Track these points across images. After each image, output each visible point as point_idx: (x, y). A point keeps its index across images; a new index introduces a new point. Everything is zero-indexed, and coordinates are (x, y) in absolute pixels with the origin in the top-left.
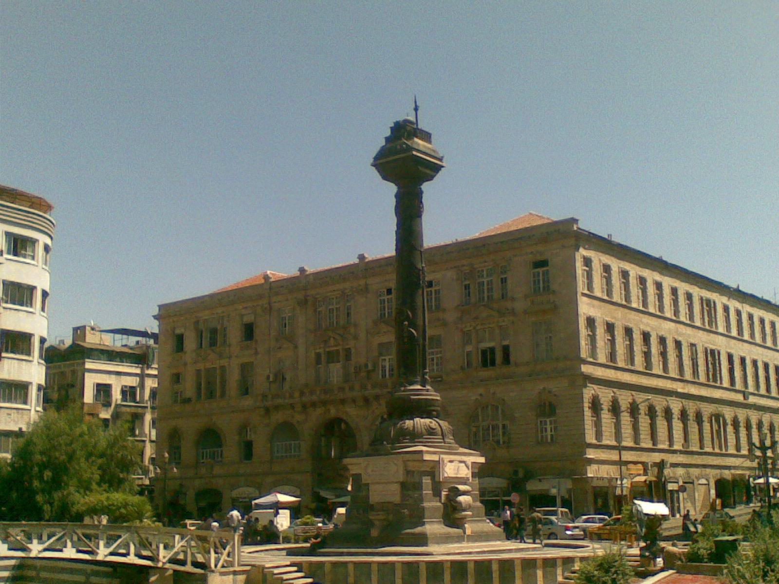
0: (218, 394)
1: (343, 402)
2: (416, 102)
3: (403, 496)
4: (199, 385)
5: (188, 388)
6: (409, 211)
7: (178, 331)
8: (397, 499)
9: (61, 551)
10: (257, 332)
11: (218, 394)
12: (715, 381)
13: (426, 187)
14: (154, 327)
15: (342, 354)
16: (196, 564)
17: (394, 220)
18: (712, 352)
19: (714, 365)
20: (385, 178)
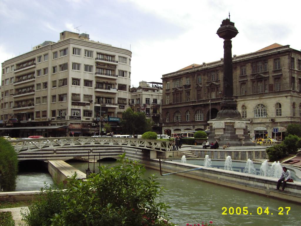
3: (224, 133)
6: (228, 47)
8: (222, 133)
9: (127, 145)
13: (233, 40)
16: (162, 150)
17: (223, 50)
20: (220, 37)
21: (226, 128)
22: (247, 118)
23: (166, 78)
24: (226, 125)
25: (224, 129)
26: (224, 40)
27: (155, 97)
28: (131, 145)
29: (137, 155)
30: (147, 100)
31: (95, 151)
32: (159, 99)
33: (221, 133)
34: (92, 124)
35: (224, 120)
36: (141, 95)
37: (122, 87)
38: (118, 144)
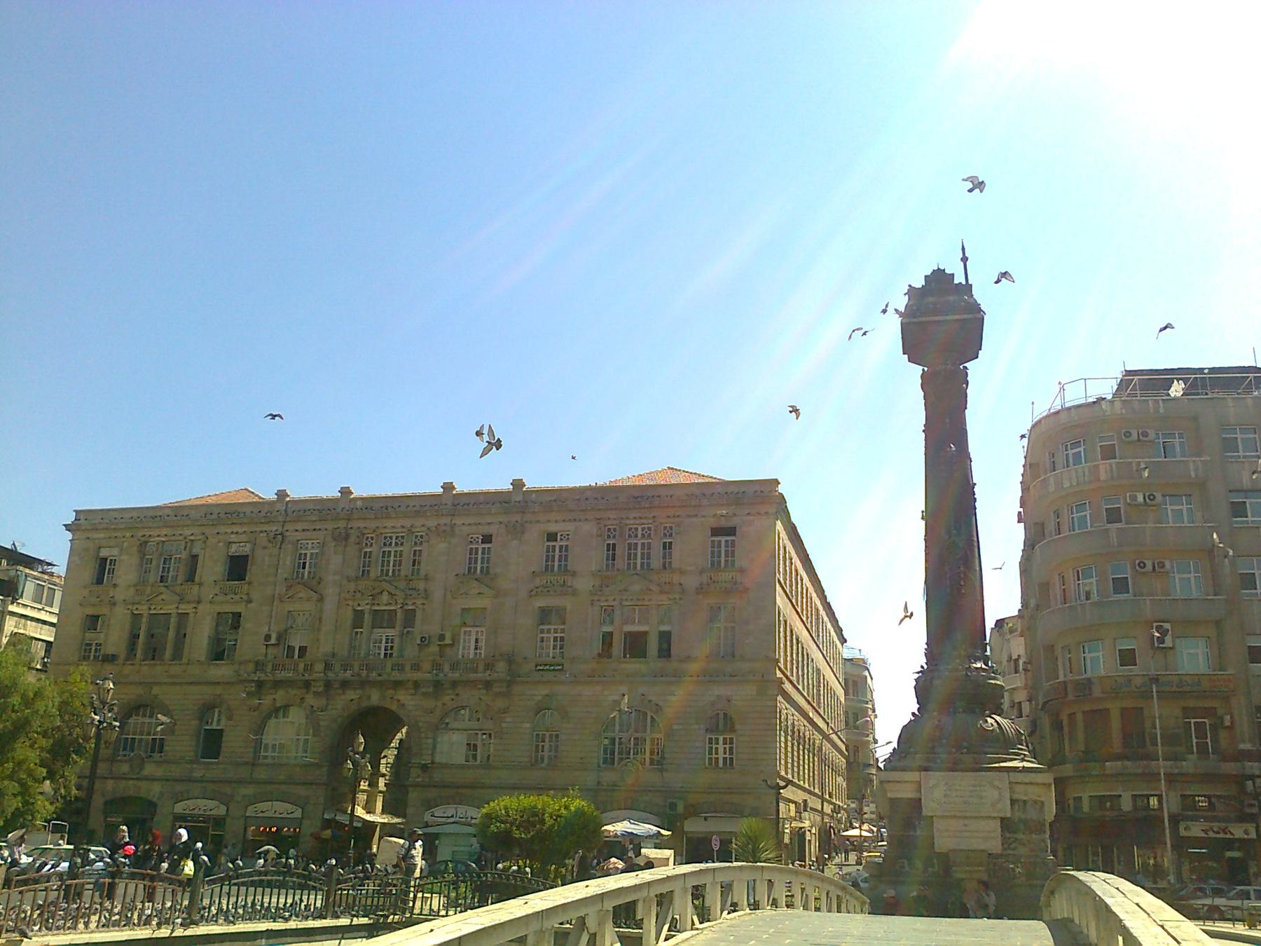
0: (168, 653)
1: (397, 684)
2: (963, 249)
4: (134, 637)
5: (114, 638)
7: (104, 553)
8: (995, 845)
10: (253, 572)
11: (168, 653)
21: (1017, 814)
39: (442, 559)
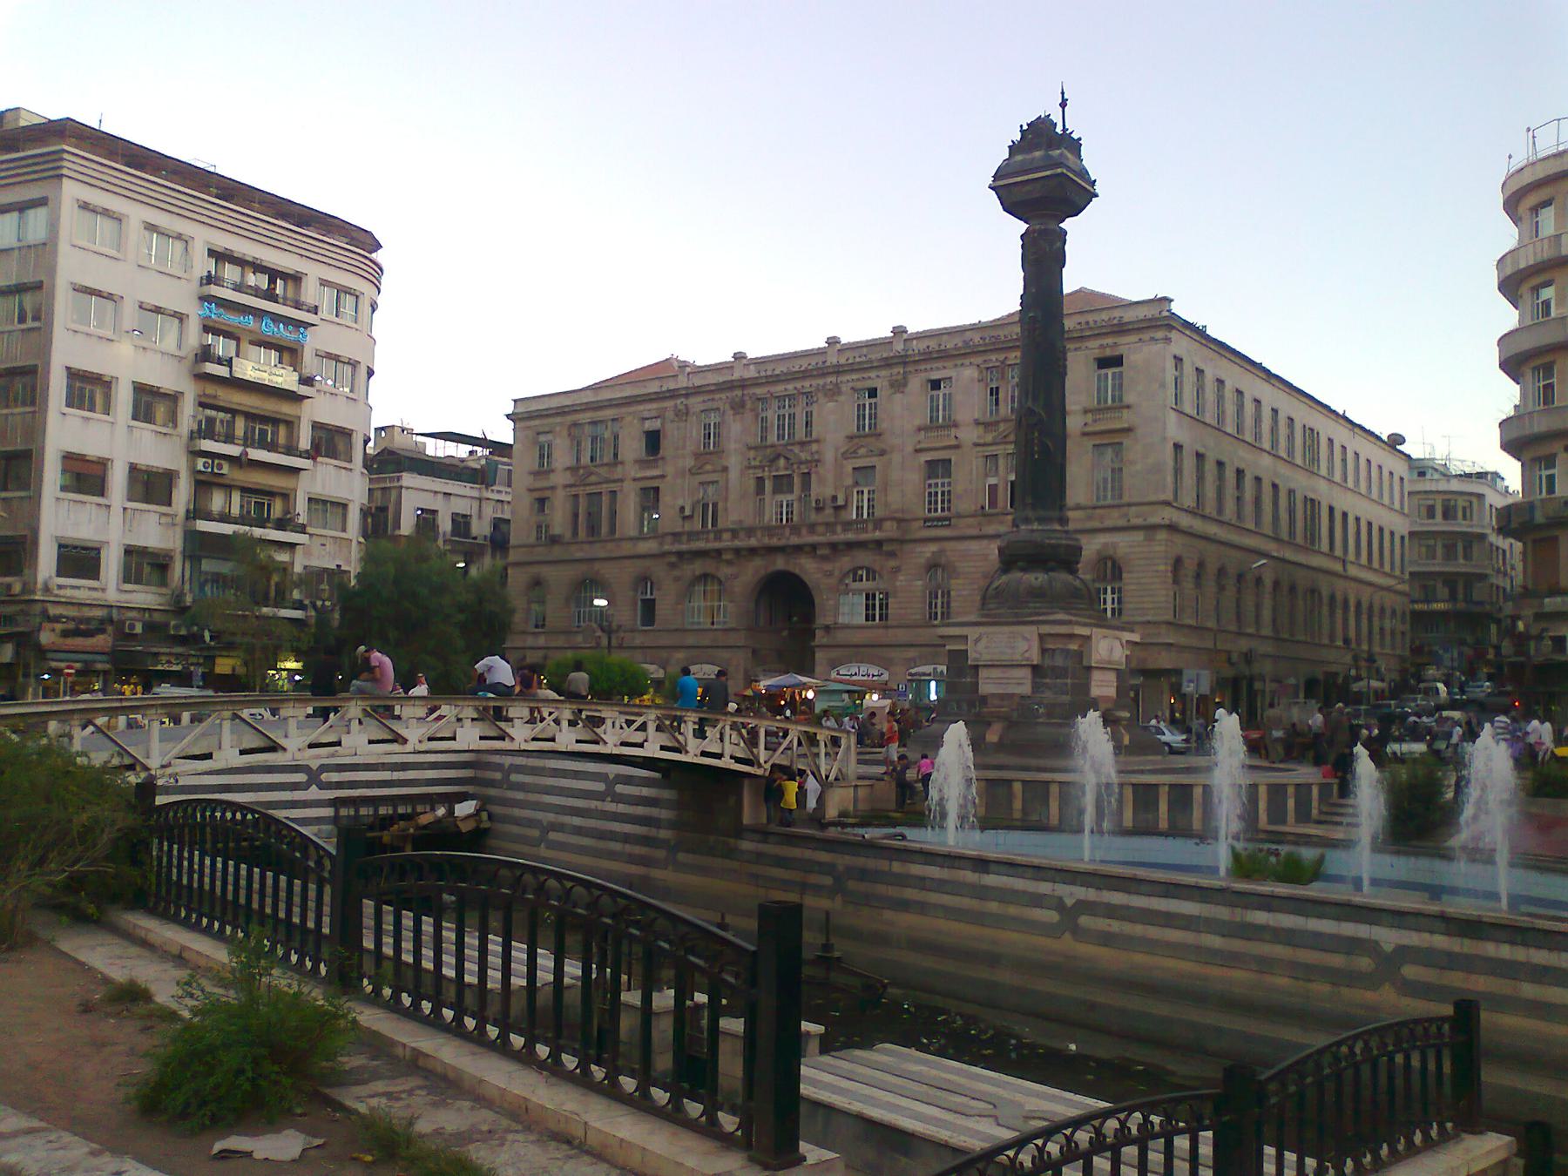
0: (604, 529)
1: (798, 549)
3: (1036, 687)
5: (558, 520)
8: (1026, 689)
9: (641, 745)
10: (667, 447)
12: (1313, 543)
14: (504, 432)
15: (797, 480)
18: (1312, 500)
19: (1313, 519)
22: (1124, 618)
23: (527, 414)
24: (1044, 651)
25: (1035, 668)
26: (1023, 227)
27: (461, 507)
28: (663, 748)
29: (619, 799)
30: (427, 519)
31: (335, 777)
32: (480, 517)
33: (1021, 683)
34: (167, 625)
35: (1032, 623)
36: (394, 494)
37: (331, 442)
38: (597, 743)
39: (834, 421)
